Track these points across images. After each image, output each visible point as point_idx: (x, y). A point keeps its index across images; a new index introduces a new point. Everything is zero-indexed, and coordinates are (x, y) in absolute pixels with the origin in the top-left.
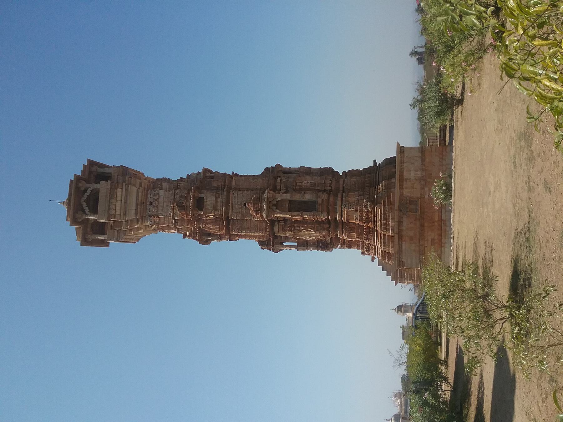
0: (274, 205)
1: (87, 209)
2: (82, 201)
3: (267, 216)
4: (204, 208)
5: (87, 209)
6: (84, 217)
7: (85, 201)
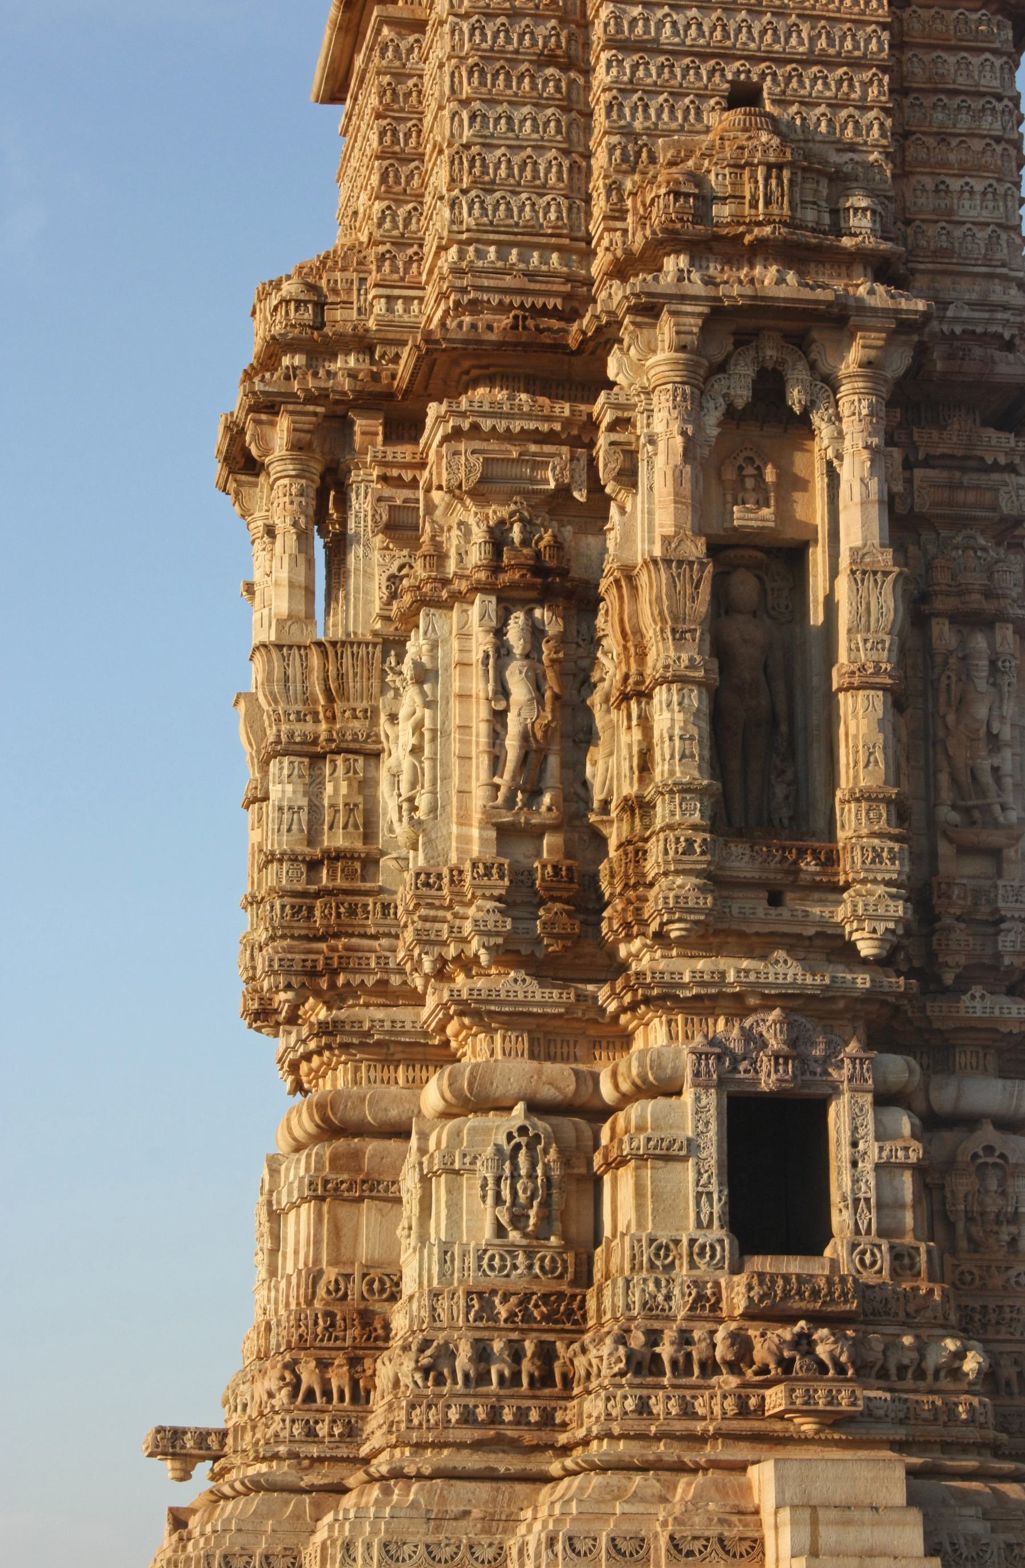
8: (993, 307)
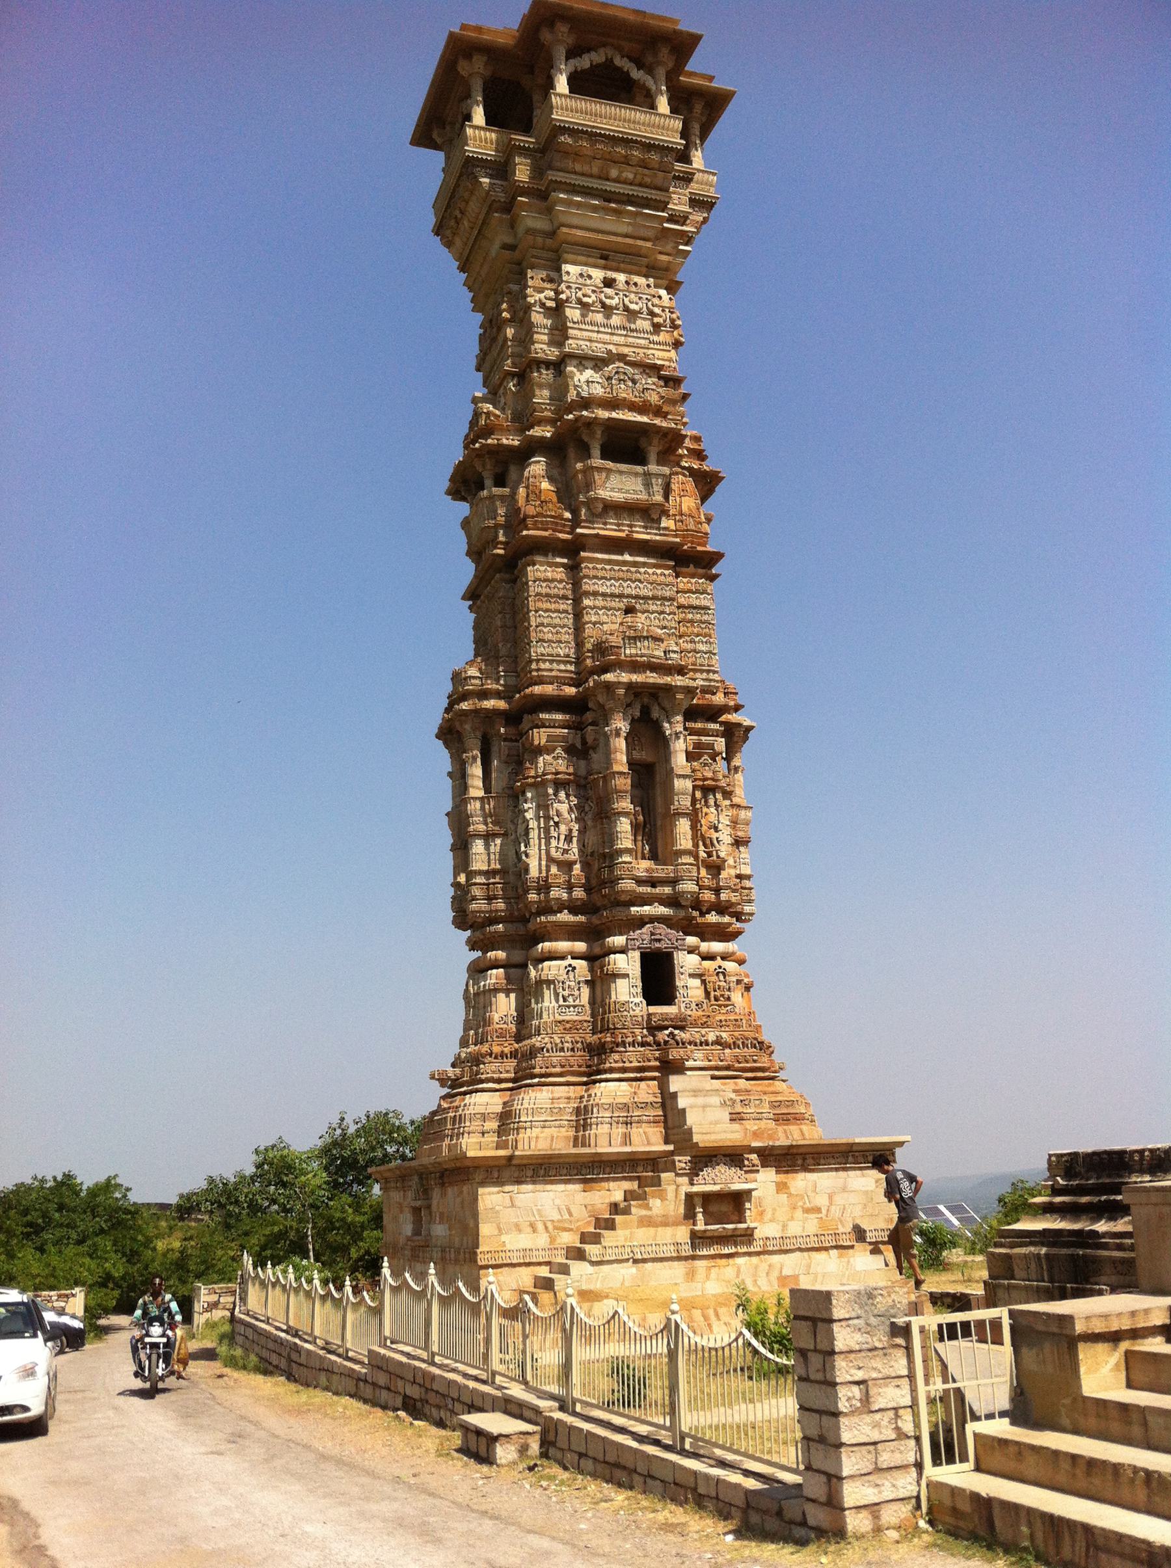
0: (645, 711)
1: (584, 62)
2: (610, 52)
3: (609, 687)
4: (610, 464)
5: (584, 62)
6: (560, 52)
7: (609, 63)
8: (711, 680)
